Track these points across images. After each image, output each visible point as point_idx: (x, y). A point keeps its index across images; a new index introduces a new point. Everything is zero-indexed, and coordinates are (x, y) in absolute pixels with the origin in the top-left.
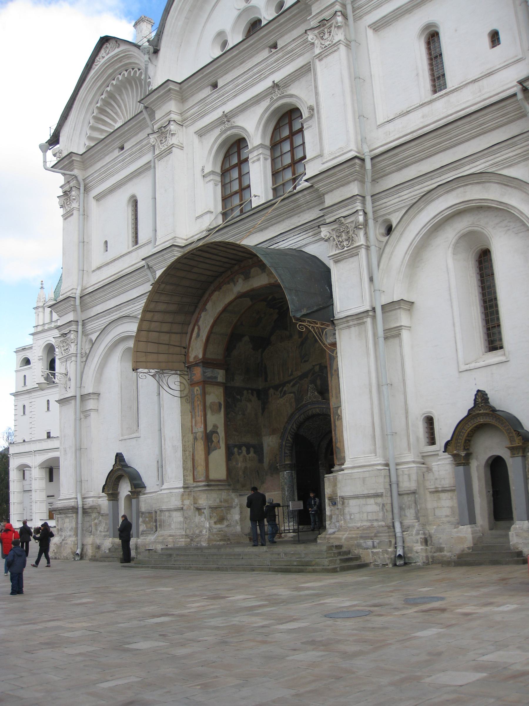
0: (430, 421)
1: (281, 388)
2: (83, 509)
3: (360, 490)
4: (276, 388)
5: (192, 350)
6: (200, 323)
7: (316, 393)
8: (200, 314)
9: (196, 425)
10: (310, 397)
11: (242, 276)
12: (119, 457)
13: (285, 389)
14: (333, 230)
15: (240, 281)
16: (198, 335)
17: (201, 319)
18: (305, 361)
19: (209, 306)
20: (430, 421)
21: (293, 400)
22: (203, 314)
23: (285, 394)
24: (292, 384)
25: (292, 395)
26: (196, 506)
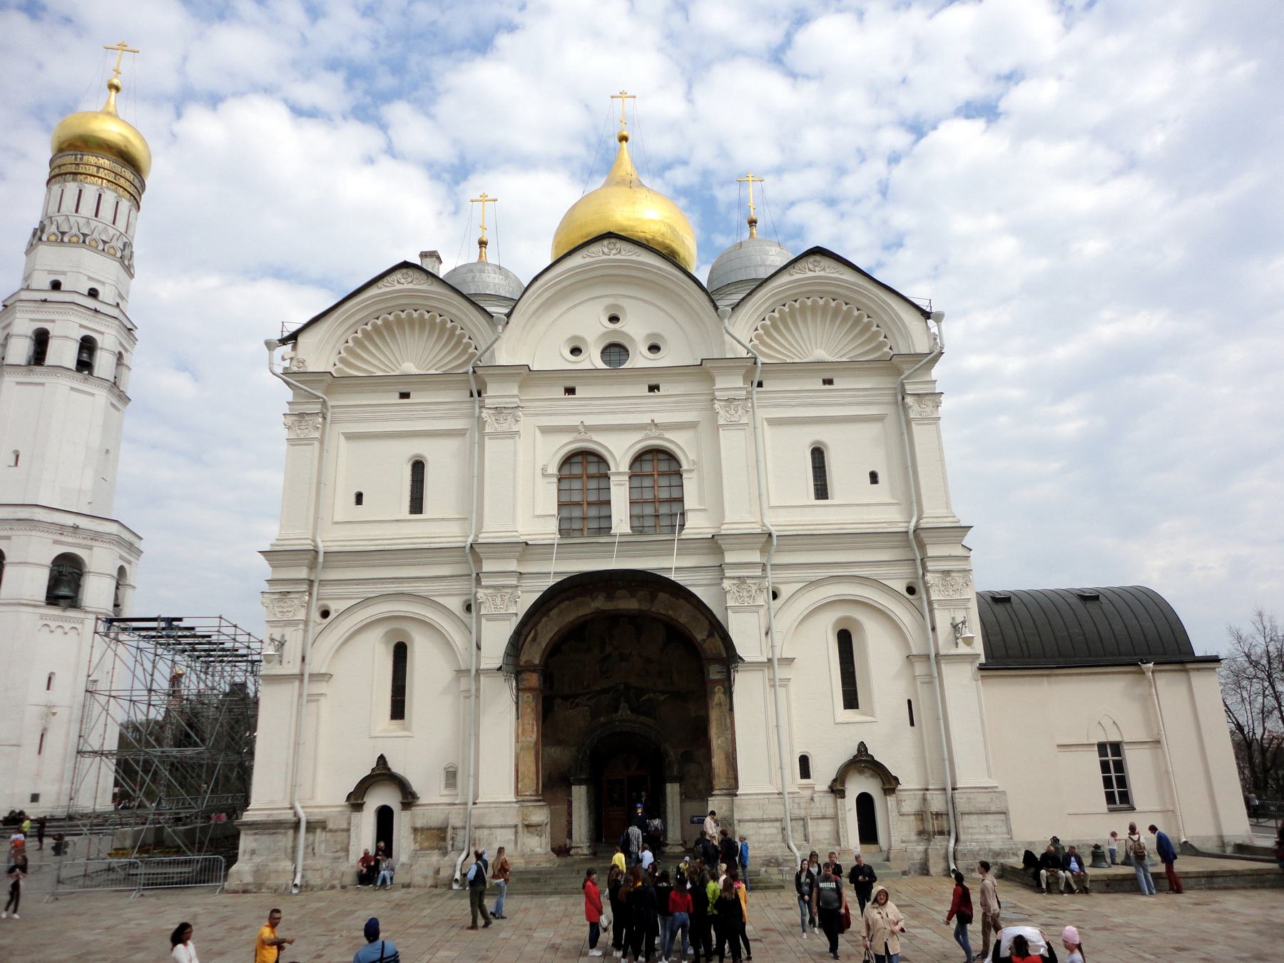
0: (804, 761)
1: (572, 699)
2: (308, 823)
3: (757, 814)
4: (565, 698)
5: (524, 653)
6: (539, 628)
7: (629, 712)
8: (541, 618)
9: (523, 734)
10: (621, 715)
11: (604, 594)
12: (382, 759)
13: (577, 700)
14: (734, 584)
15: (600, 597)
16: (534, 639)
17: (541, 624)
18: (606, 678)
19: (554, 613)
20: (804, 761)
21: (588, 713)
22: (544, 620)
23: (577, 705)
24: (587, 697)
25: (587, 708)
26: (526, 823)
